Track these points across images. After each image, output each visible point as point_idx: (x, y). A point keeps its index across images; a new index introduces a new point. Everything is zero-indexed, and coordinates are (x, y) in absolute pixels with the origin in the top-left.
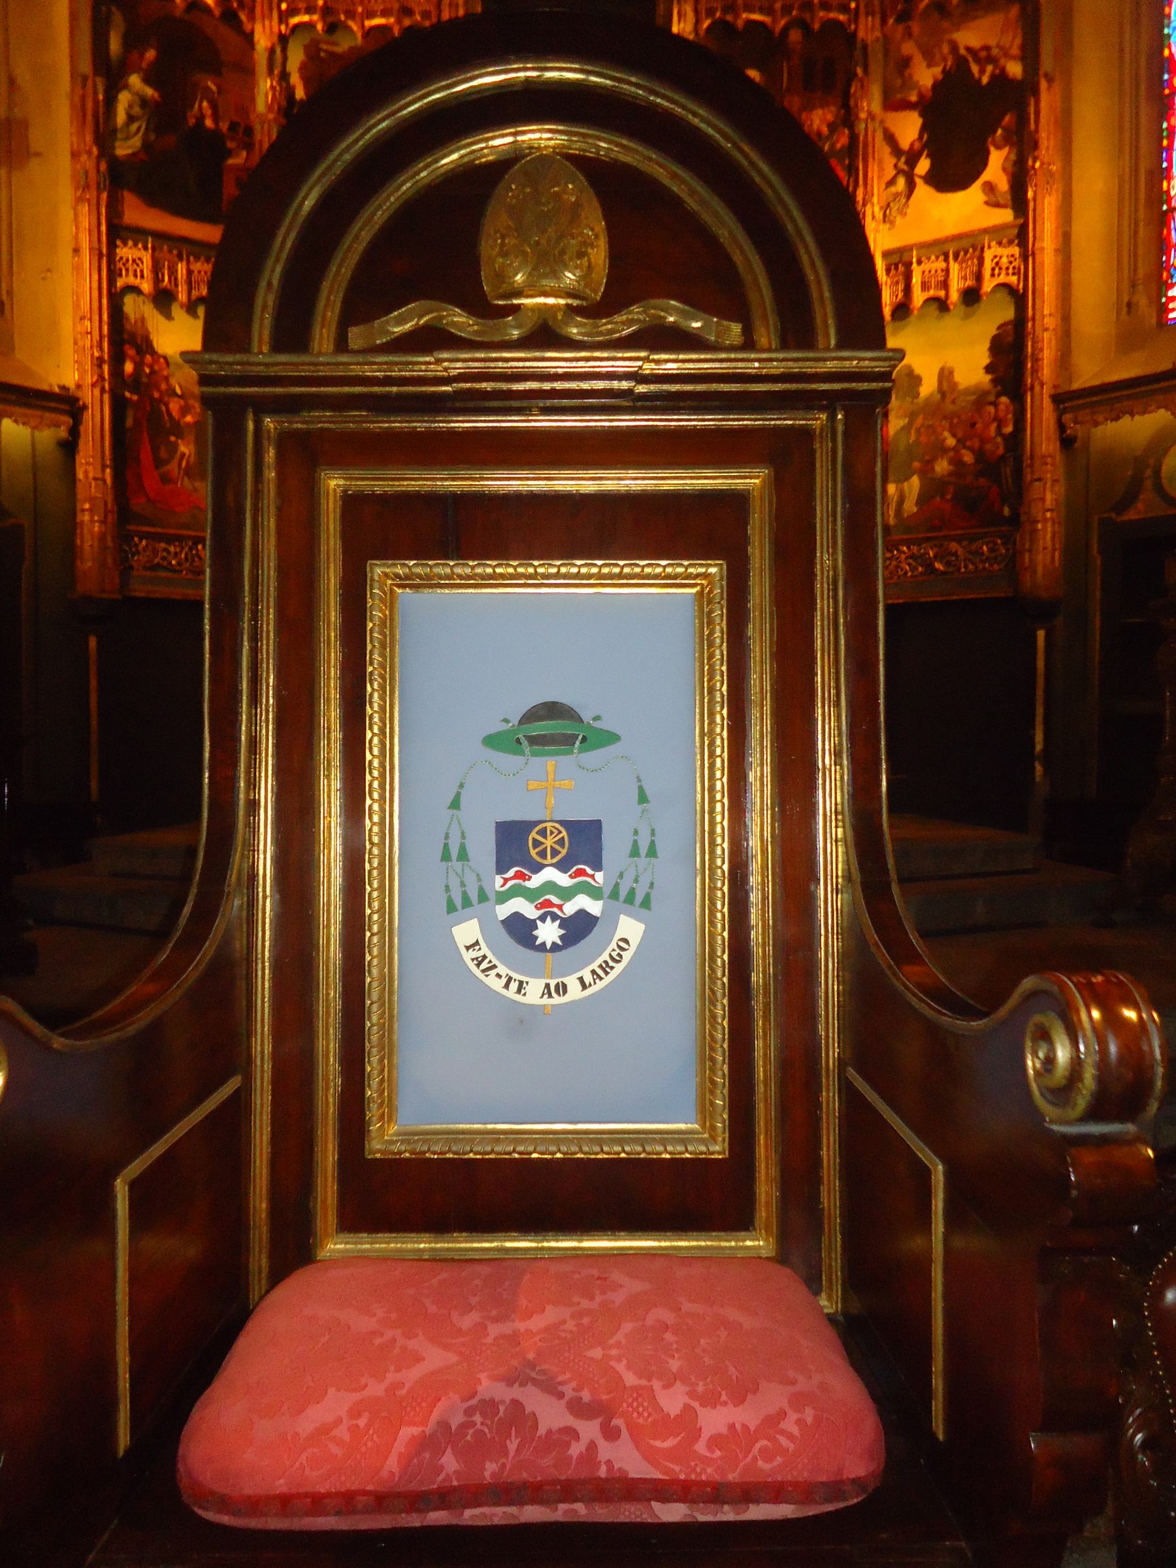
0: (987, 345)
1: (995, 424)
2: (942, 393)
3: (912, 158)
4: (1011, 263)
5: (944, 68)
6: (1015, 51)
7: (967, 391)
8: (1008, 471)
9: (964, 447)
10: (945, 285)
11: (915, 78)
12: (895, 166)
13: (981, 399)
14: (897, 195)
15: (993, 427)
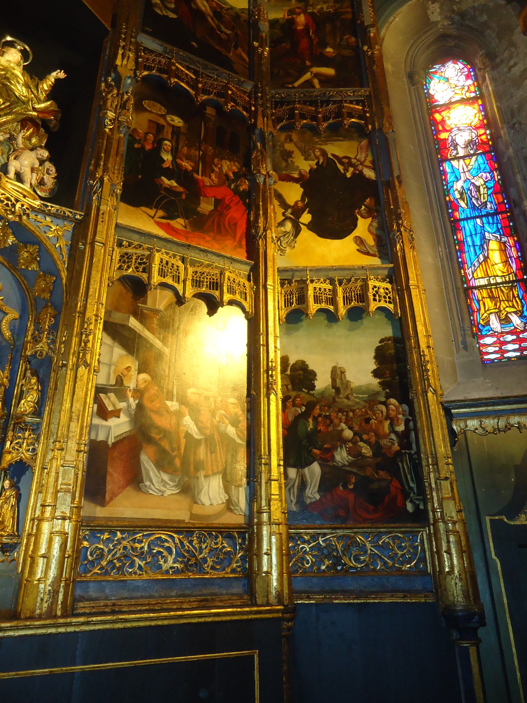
0: (373, 354)
1: (389, 421)
2: (338, 390)
3: (297, 212)
4: (387, 294)
5: (318, 162)
6: (367, 163)
7: (359, 390)
8: (405, 466)
9: (362, 440)
10: (333, 301)
11: (295, 164)
12: (284, 214)
13: (372, 400)
14: (285, 233)
15: (387, 424)
